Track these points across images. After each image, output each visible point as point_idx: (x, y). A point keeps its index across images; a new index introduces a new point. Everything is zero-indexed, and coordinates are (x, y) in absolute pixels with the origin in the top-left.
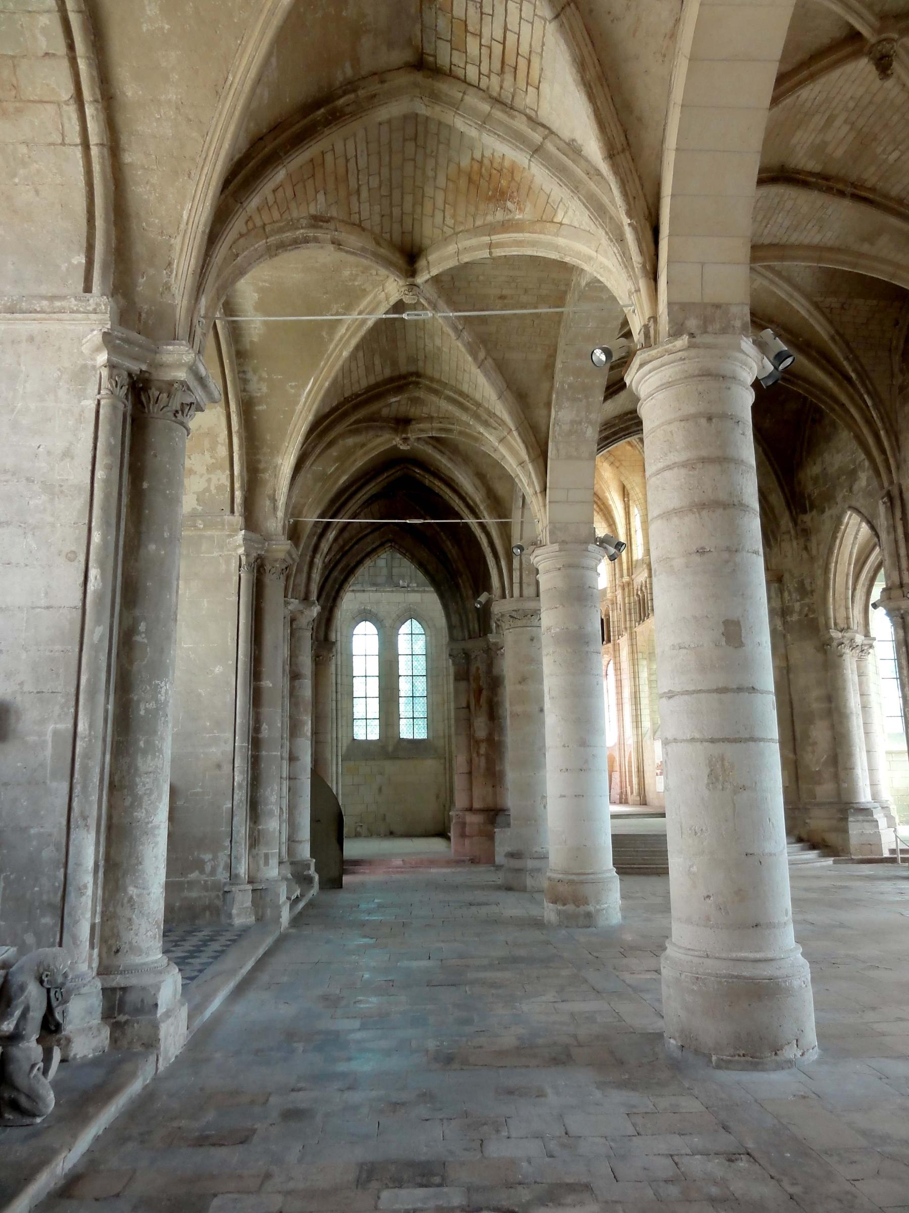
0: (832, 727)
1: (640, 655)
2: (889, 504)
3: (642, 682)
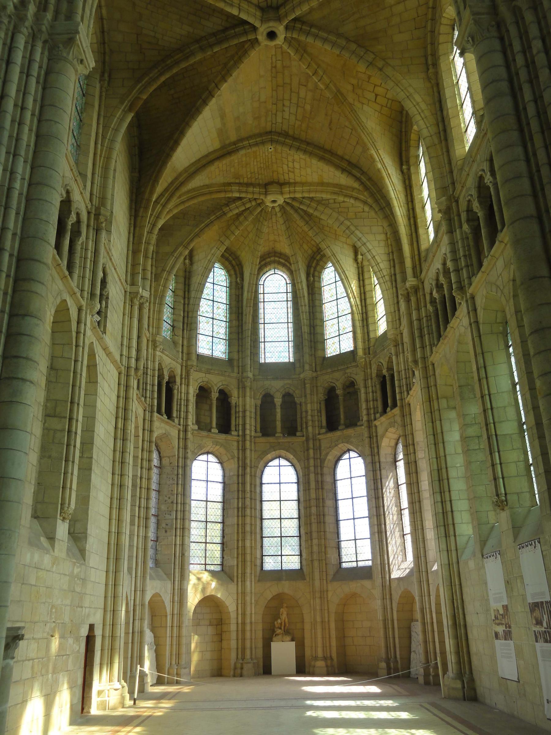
1: (443, 403)
3: (450, 449)
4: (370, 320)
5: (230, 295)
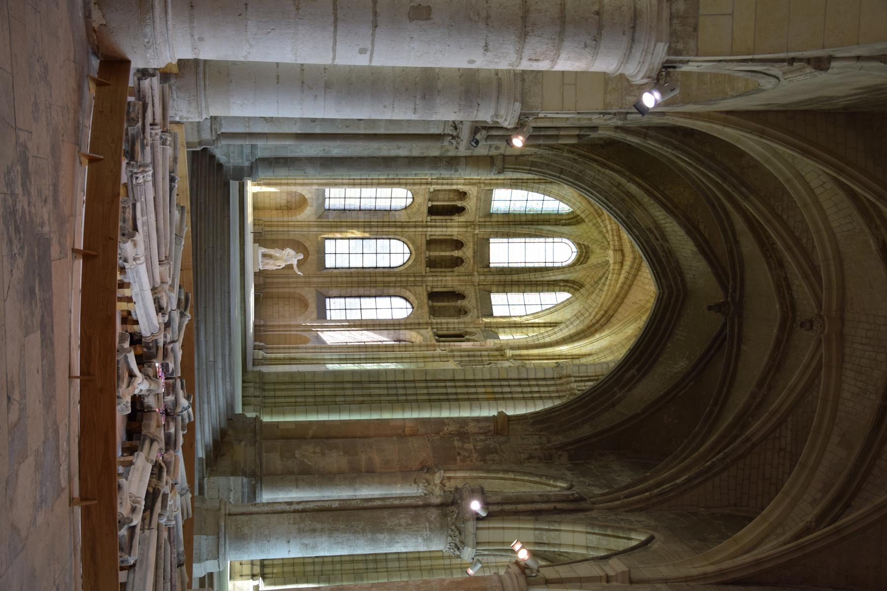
0: (341, 472)
2: (571, 497)
4: (514, 330)
5: (549, 214)
